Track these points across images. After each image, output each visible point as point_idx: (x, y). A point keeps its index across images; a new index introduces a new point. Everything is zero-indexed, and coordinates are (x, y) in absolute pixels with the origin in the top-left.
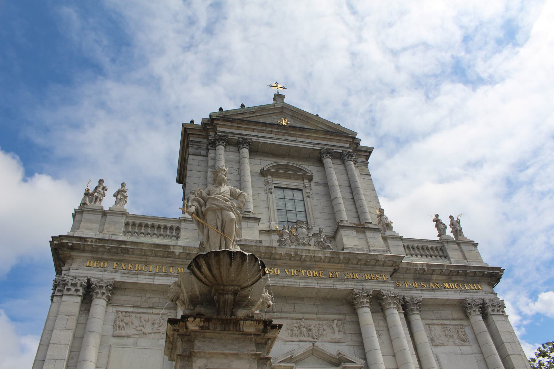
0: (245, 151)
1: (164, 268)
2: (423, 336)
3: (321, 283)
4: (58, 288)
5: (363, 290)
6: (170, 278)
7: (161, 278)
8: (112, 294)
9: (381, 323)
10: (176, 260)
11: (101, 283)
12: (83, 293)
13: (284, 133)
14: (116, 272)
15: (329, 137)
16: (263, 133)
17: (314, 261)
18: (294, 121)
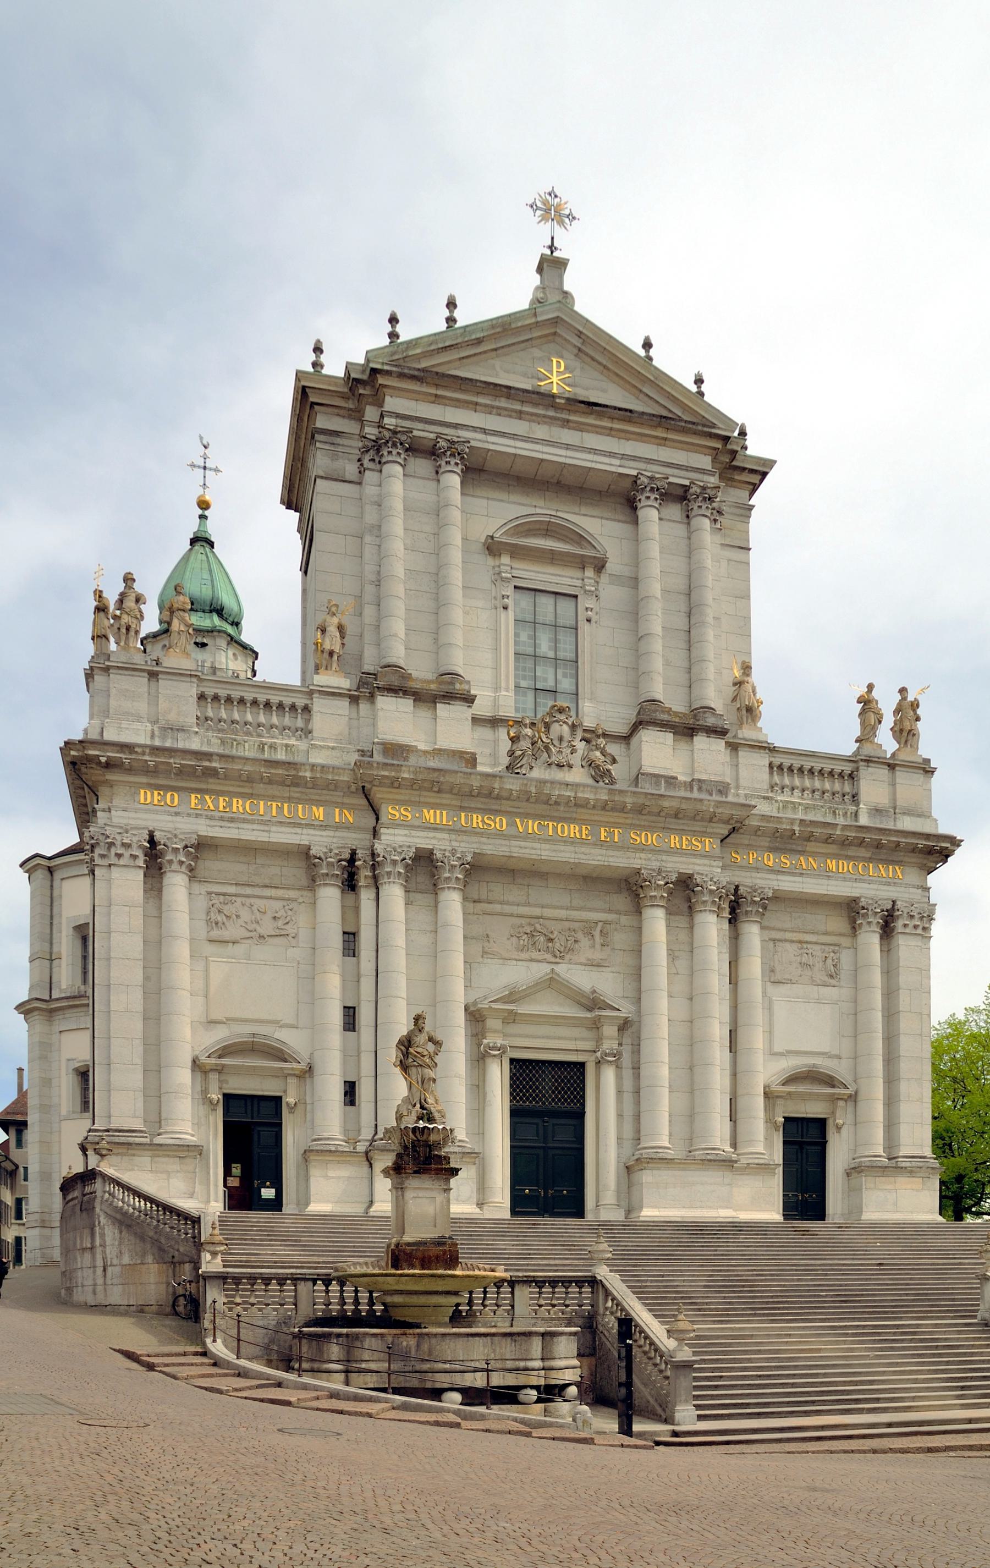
0: (454, 481)
1: (286, 805)
2: (753, 966)
3: (583, 853)
4: (98, 851)
5: (660, 871)
6: (299, 830)
7: (283, 829)
8: (196, 858)
9: (683, 936)
10: (307, 791)
11: (175, 840)
12: (145, 861)
13: (551, 418)
14: (197, 816)
15: (660, 433)
16: (500, 415)
17: (575, 805)
18: (582, 368)
